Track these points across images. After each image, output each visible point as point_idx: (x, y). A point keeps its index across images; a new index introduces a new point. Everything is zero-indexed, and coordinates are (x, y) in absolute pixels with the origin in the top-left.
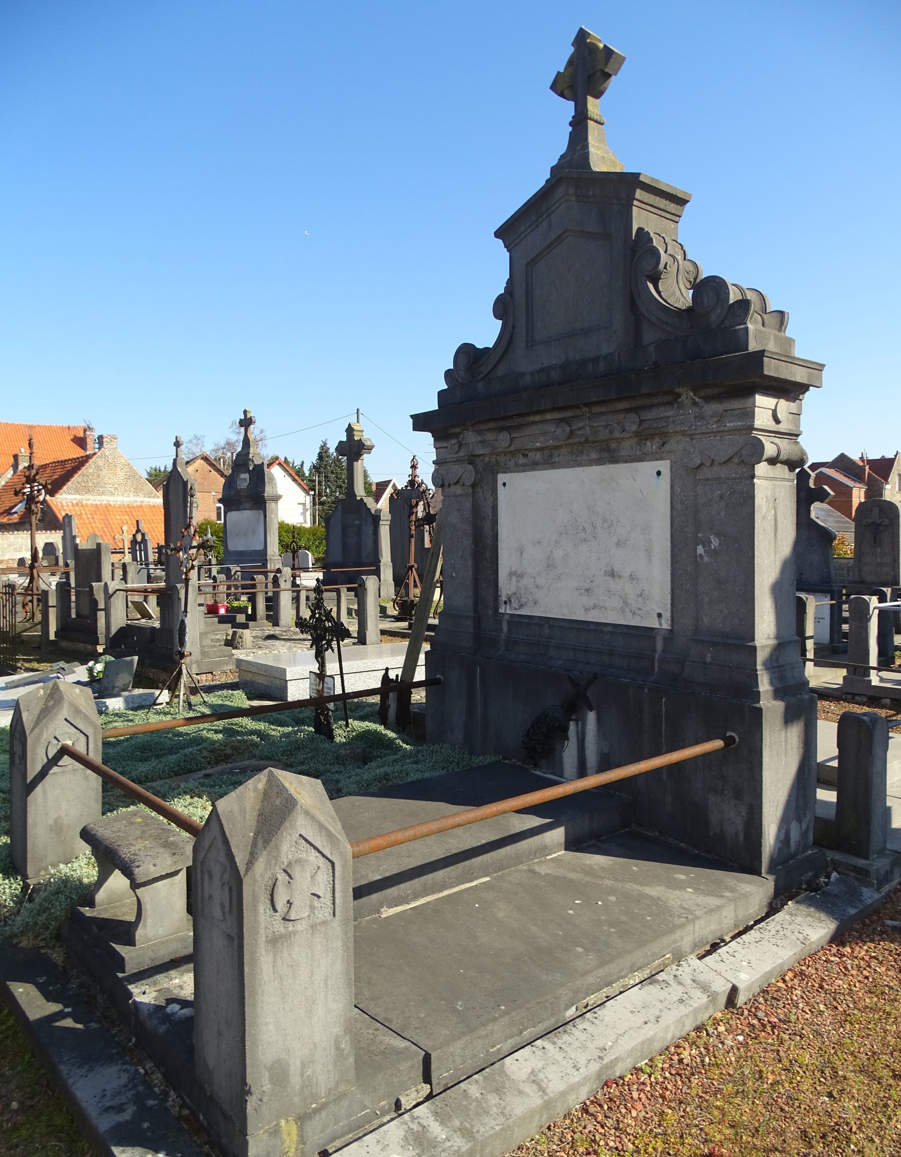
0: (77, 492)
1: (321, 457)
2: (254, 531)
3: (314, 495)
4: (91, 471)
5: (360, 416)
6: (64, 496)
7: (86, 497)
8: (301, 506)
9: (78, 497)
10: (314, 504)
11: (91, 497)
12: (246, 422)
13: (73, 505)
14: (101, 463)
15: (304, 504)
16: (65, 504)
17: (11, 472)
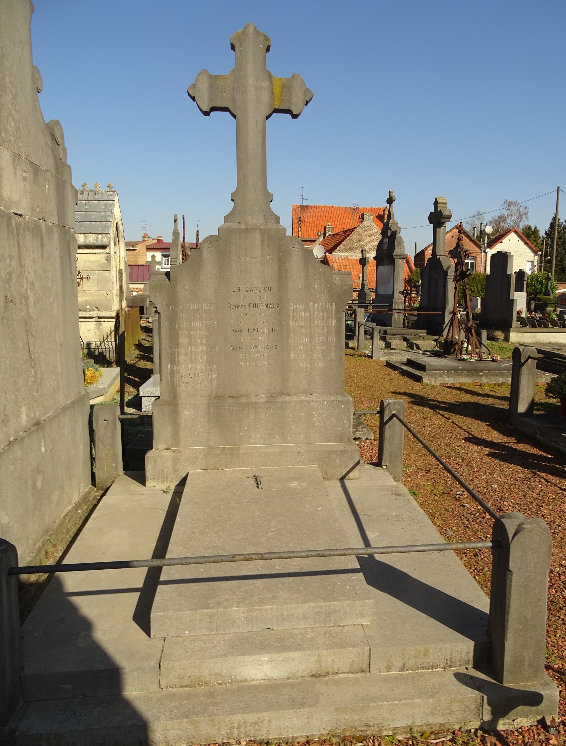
0: (346, 251)
1: (552, 226)
2: (389, 281)
3: (541, 256)
4: (355, 237)
5: (560, 192)
6: (338, 253)
7: (351, 254)
8: (530, 263)
9: (346, 254)
10: (541, 262)
11: (354, 254)
12: (390, 201)
13: (342, 260)
14: (362, 232)
15: (533, 262)
16: (337, 259)
17: (322, 238)
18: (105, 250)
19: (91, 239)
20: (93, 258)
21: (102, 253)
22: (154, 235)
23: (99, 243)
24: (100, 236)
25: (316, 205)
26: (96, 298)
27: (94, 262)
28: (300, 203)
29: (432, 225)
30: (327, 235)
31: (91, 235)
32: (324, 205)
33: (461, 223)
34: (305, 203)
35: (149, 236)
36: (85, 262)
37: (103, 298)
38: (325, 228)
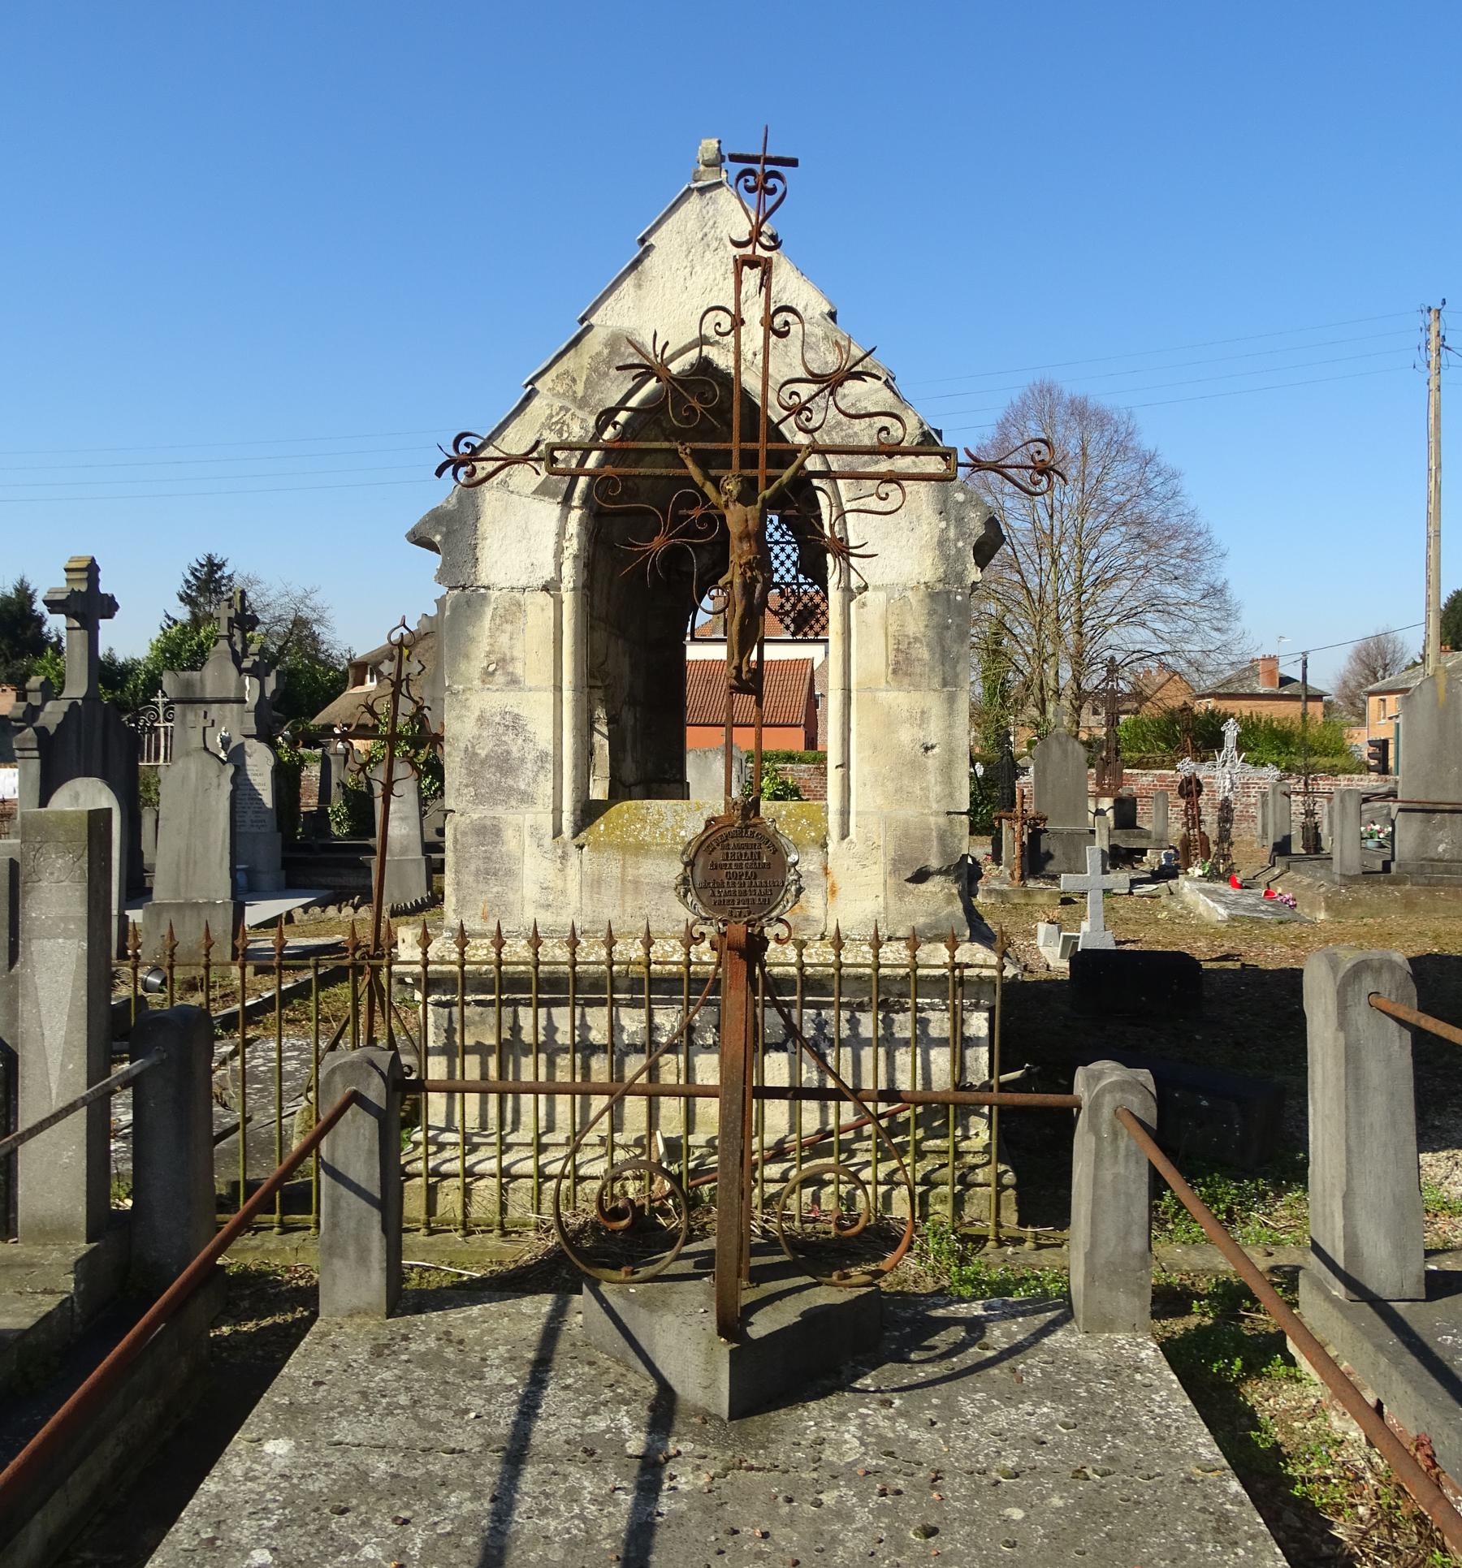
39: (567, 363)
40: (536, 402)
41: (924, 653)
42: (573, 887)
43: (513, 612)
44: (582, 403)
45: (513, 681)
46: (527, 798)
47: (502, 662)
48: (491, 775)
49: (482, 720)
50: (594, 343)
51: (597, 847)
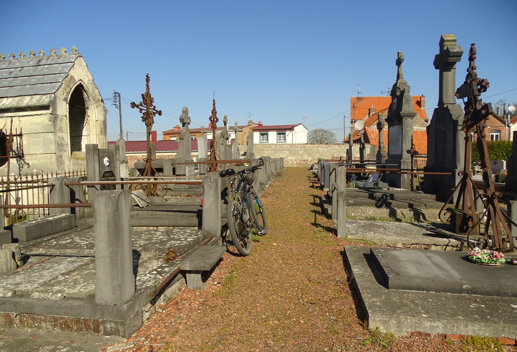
18: (47, 111)
19: (35, 101)
20: (38, 119)
21: (46, 114)
22: (256, 121)
23: (41, 103)
24: (45, 96)
25: (368, 96)
26: (41, 161)
27: (39, 123)
28: (356, 95)
29: (438, 70)
30: (371, 115)
31: (37, 96)
32: (374, 96)
33: (473, 45)
34: (360, 96)
35: (211, 114)
36: (31, 124)
37: (48, 161)
38: (369, 110)
39: (66, 79)
40: (63, 85)
41: (103, 130)
42: (71, 165)
43: (61, 120)
44: (68, 86)
45: (62, 131)
46: (65, 151)
47: (61, 128)
48: (61, 147)
49: (59, 138)
50: (69, 77)
51: (74, 159)
